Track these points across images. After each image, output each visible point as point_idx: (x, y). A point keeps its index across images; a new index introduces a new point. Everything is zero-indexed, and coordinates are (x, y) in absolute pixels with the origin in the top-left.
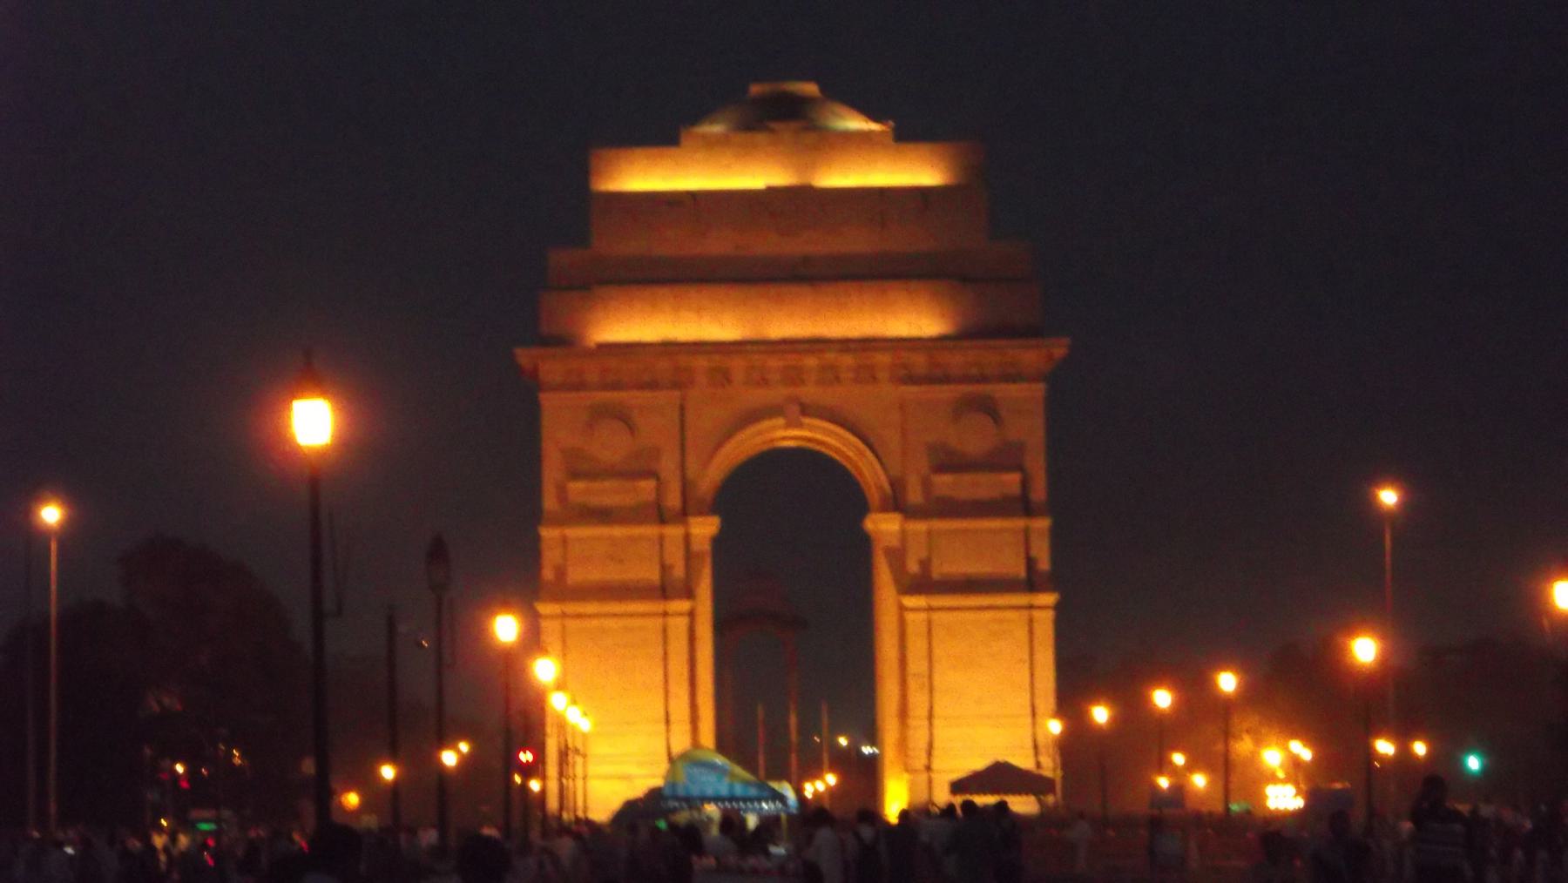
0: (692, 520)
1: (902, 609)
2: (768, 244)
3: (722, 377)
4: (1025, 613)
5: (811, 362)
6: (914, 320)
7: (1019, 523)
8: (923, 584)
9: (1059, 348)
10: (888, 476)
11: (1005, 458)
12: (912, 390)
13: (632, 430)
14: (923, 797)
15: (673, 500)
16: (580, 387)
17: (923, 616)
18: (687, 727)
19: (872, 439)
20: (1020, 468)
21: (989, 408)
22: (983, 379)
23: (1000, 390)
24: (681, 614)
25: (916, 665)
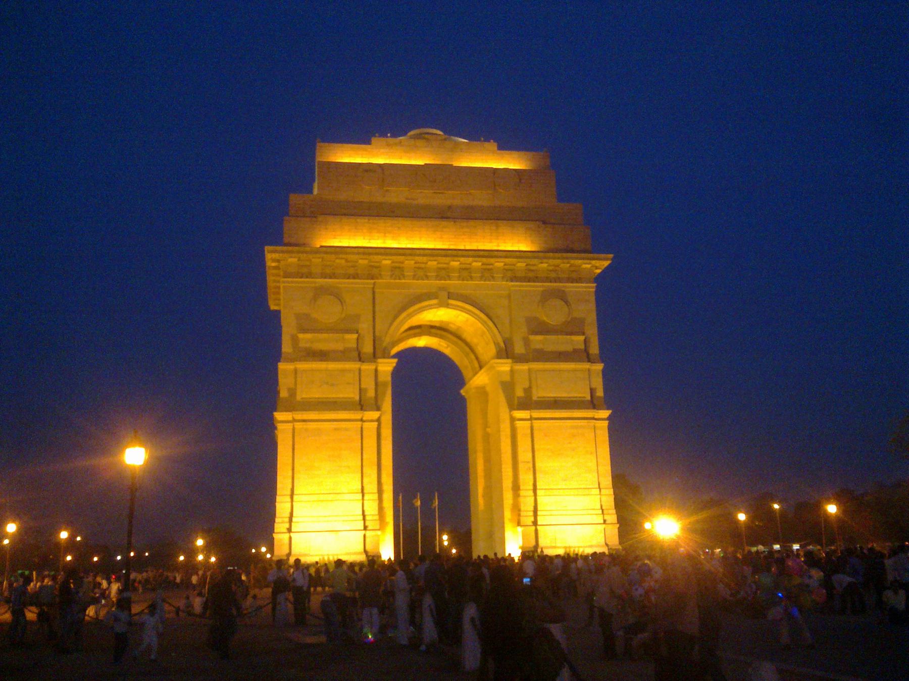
0: (380, 360)
1: (513, 420)
2: (424, 197)
3: (397, 271)
5: (455, 264)
6: (517, 242)
7: (587, 366)
8: (526, 403)
10: (503, 338)
11: (572, 327)
13: (342, 302)
14: (532, 543)
15: (368, 348)
16: (309, 275)
18: (376, 496)
20: (583, 334)
21: (562, 296)
22: (558, 280)
24: (372, 421)
25: (524, 455)
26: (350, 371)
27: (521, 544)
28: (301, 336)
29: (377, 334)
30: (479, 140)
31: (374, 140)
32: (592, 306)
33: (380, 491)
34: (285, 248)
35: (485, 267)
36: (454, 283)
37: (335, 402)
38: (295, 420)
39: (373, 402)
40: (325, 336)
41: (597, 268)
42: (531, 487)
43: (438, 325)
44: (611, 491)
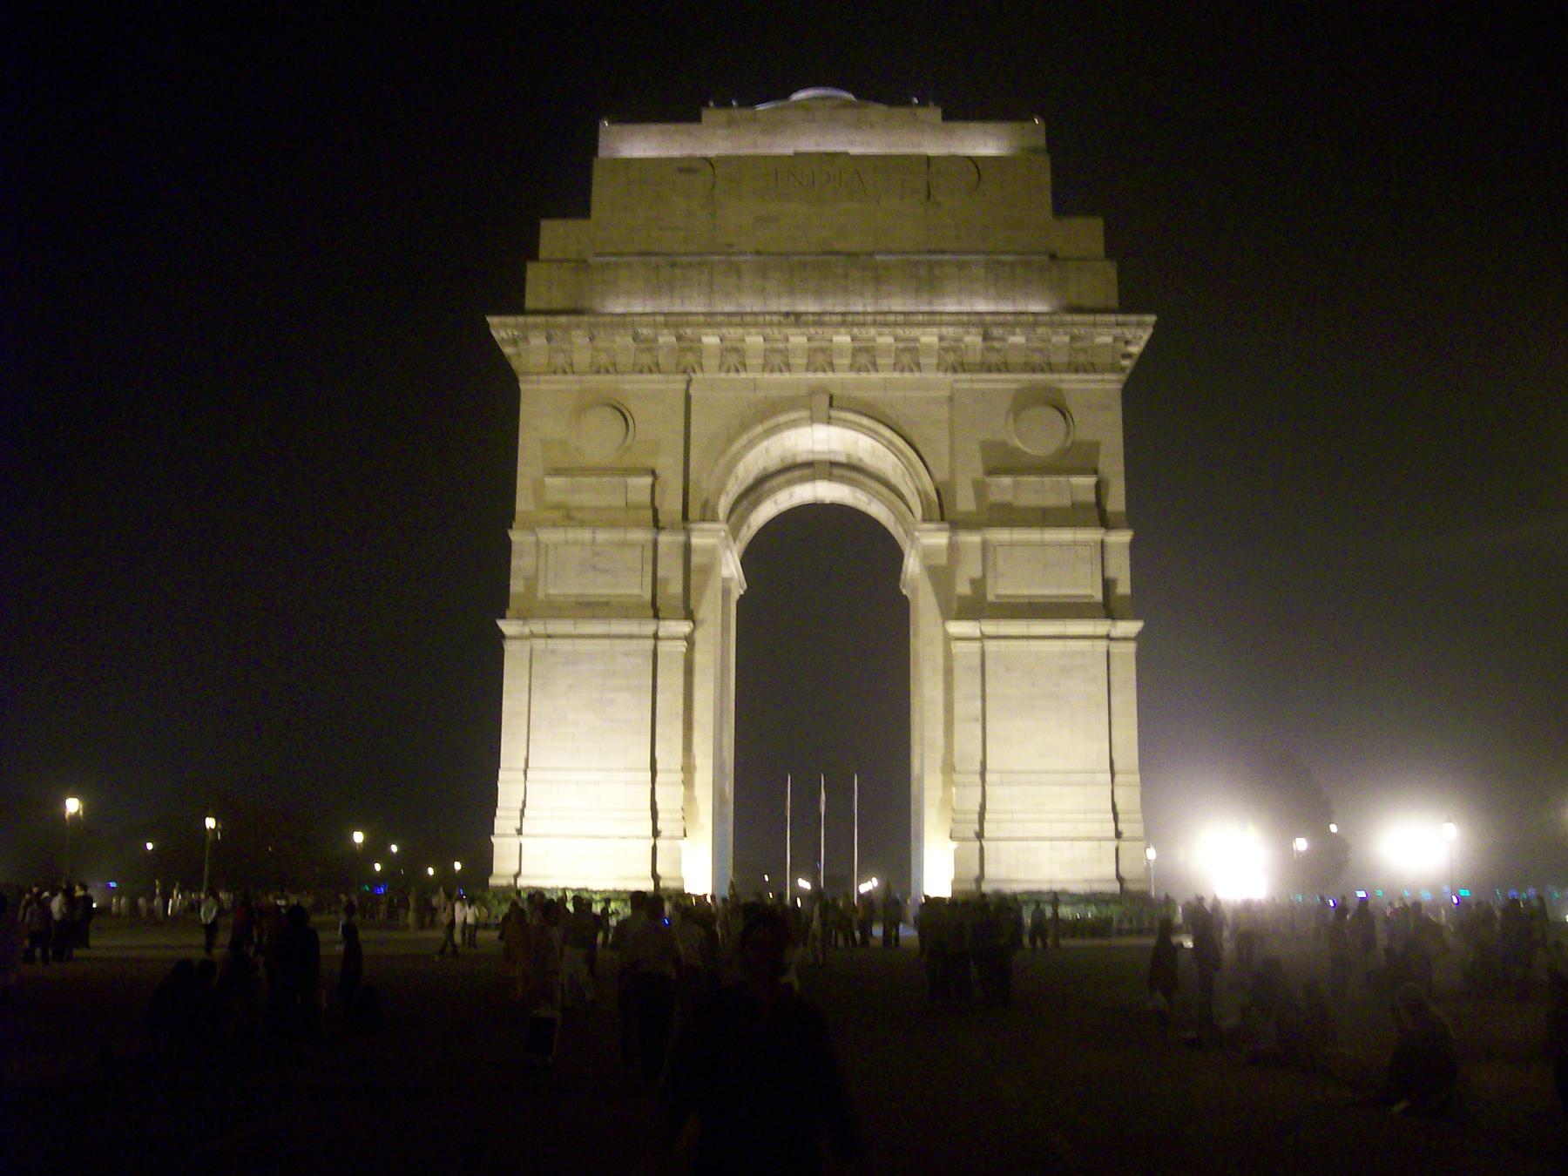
0: (693, 526)
1: (949, 639)
3: (734, 357)
4: (1102, 645)
7: (1093, 535)
9: (1138, 334)
12: (965, 381)
15: (671, 504)
16: (568, 369)
17: (976, 646)
18: (680, 776)
19: (915, 438)
20: (1095, 472)
22: (1050, 368)
23: (1070, 383)
25: (967, 706)
26: (632, 545)
27: (952, 876)
28: (549, 481)
29: (692, 476)
30: (910, 103)
31: (707, 114)
32: (1115, 417)
33: (688, 769)
34: (521, 319)
35: (901, 345)
36: (842, 378)
37: (607, 604)
38: (533, 635)
39: (680, 603)
40: (594, 480)
41: (1127, 343)
42: (978, 767)
43: (843, 459)
44: (1136, 778)
